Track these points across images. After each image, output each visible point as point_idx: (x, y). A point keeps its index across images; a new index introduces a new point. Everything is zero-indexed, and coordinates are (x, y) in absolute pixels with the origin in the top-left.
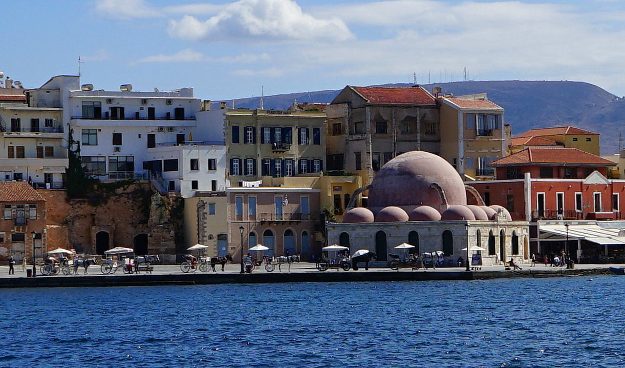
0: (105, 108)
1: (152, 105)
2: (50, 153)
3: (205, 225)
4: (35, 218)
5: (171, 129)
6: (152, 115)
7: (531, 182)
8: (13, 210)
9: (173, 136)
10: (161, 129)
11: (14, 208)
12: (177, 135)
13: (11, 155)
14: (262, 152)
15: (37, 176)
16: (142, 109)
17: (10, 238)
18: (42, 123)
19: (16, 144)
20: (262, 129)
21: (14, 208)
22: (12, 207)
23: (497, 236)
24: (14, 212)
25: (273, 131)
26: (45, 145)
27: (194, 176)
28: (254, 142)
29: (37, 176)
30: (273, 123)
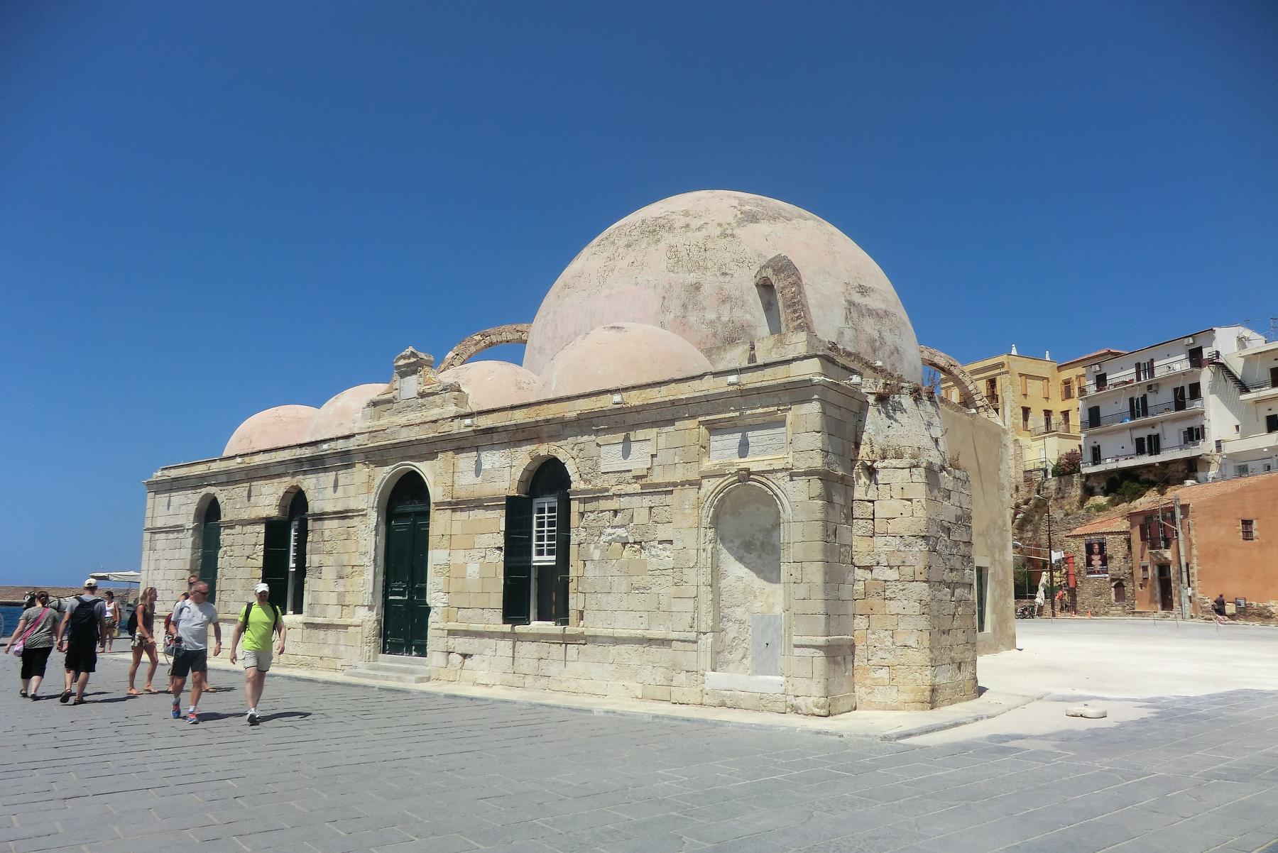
23: (343, 515)
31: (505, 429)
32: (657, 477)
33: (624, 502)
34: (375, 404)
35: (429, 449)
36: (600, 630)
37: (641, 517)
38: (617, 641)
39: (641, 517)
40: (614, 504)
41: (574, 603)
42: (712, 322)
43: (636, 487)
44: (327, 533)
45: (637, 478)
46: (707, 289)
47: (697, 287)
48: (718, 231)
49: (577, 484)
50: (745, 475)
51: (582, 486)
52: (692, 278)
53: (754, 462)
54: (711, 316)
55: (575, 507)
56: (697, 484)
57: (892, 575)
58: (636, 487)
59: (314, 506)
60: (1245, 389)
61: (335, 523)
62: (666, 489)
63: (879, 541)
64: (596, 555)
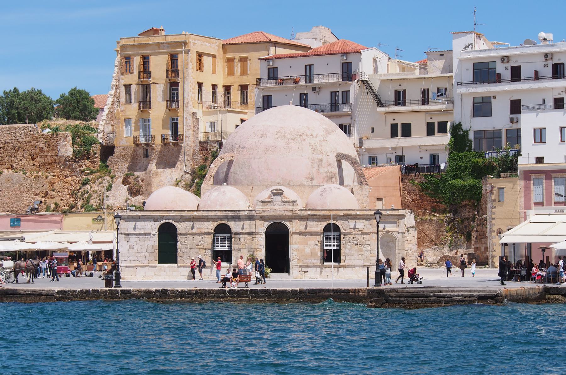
1: (559, 60)
2: (442, 128)
3: (493, 216)
13: (394, 134)
15: (421, 158)
16: (546, 66)
18: (432, 91)
19: (400, 120)
23: (250, 234)
26: (436, 120)
27: (540, 150)
29: (421, 158)
31: (319, 215)
32: (366, 231)
33: (356, 236)
34: (262, 202)
35: (291, 218)
36: (351, 264)
37: (361, 239)
38: (355, 266)
39: (361, 239)
40: (354, 236)
41: (342, 258)
42: (326, 172)
43: (360, 232)
44: (242, 239)
45: (360, 230)
46: (324, 161)
47: (321, 160)
48: (322, 139)
49: (342, 231)
50: (388, 232)
51: (344, 231)
52: (320, 157)
53: (387, 229)
54: (326, 170)
55: (342, 236)
57: (411, 252)
59: (234, 230)
61: (246, 236)
63: (409, 245)
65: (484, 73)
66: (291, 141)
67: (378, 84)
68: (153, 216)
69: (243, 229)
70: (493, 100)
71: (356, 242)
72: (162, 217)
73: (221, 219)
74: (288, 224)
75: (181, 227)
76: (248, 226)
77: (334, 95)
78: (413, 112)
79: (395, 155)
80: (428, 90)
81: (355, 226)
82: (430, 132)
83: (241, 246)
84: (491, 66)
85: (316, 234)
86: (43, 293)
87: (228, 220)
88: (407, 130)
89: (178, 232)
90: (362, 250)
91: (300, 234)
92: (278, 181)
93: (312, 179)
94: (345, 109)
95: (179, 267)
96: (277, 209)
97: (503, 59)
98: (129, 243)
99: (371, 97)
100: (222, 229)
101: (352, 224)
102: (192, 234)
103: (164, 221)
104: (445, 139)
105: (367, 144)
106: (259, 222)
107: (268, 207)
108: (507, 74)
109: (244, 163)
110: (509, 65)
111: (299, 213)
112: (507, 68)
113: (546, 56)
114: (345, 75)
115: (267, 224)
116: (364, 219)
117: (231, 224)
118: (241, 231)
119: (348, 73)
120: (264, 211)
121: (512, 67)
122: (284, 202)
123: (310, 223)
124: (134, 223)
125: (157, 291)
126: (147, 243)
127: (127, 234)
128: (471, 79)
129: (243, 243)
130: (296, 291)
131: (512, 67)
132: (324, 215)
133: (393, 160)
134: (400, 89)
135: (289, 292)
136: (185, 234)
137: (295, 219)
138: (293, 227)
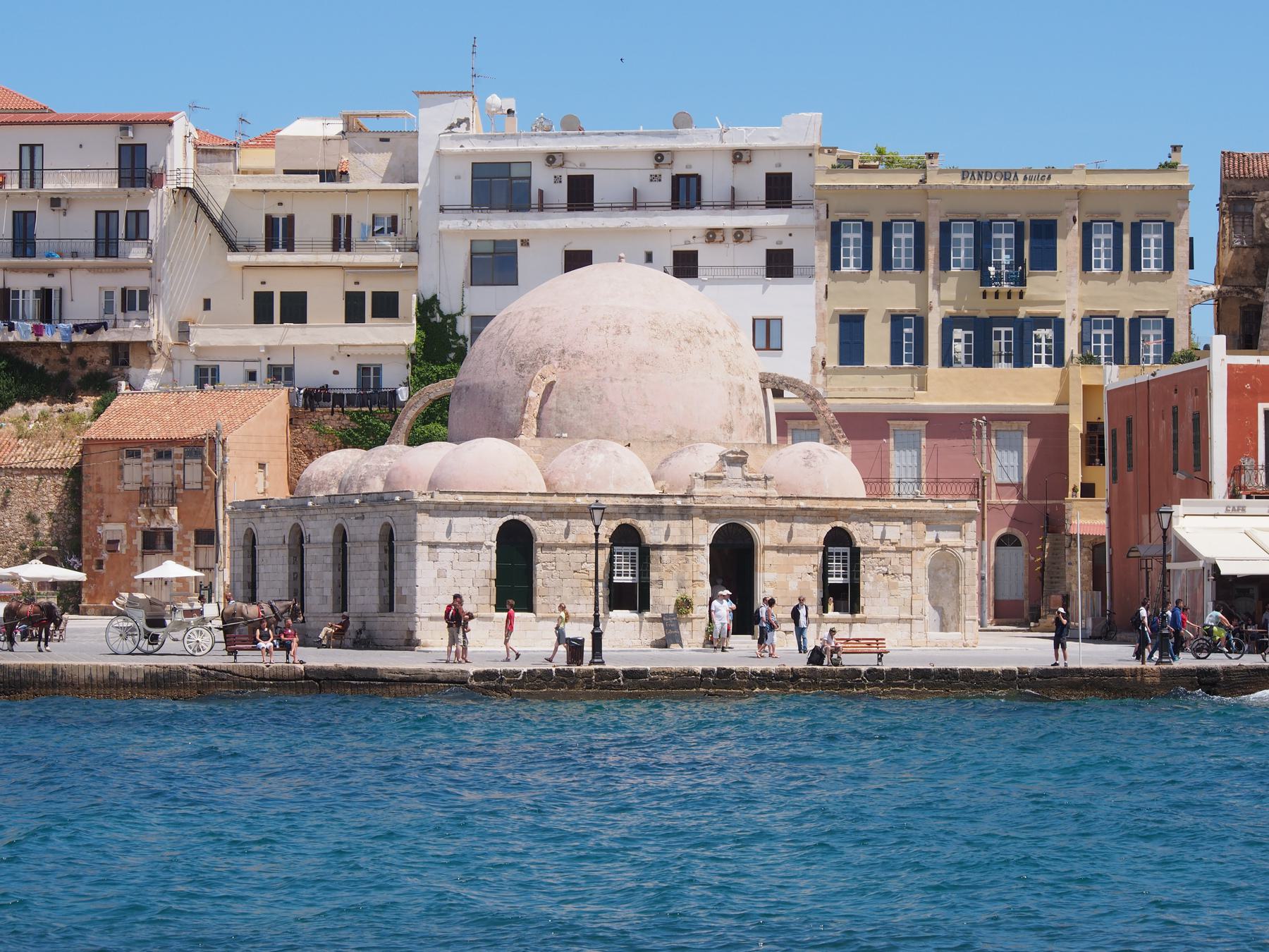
0: (542, 179)
1: (688, 167)
2: (387, 306)
4: (199, 486)
5: (740, 235)
6: (686, 192)
7: (1230, 367)
8: (145, 465)
9: (755, 256)
10: (712, 235)
11: (147, 459)
12: (771, 254)
14: (945, 295)
15: (336, 372)
16: (655, 178)
17: (138, 541)
18: (361, 221)
19: (278, 285)
20: (945, 228)
21: (147, 459)
22: (144, 455)
23: (682, 548)
24: (147, 468)
25: (983, 232)
26: (369, 287)
28: (920, 264)
29: (336, 372)
30: (985, 209)
31: (817, 510)
32: (903, 544)
33: (885, 555)
34: (706, 478)
35: (761, 515)
38: (884, 621)
39: (895, 562)
43: (893, 548)
44: (665, 559)
45: (893, 544)
50: (944, 548)
53: (943, 541)
56: (922, 549)
58: (893, 548)
60: (233, 247)
61: (675, 553)
62: (909, 551)
64: (871, 579)
65: (498, 186)
66: (684, 344)
67: (225, 200)
68: (489, 504)
69: (667, 536)
70: (521, 250)
71: (885, 569)
72: (506, 508)
73: (625, 515)
74: (755, 528)
75: (543, 531)
76: (678, 531)
77: (105, 219)
78: (310, 267)
79: (265, 363)
80: (349, 218)
81: (884, 533)
82: (354, 311)
83: (663, 575)
84: (515, 172)
85: (811, 550)
86: (440, 676)
87: (638, 517)
88: (295, 309)
89: (539, 541)
90: (895, 586)
91: (779, 549)
92: (668, 432)
93: (731, 429)
94: (137, 253)
95: (539, 620)
96: (735, 493)
97: (551, 158)
98: (438, 565)
99: (205, 226)
100: (627, 536)
101: (877, 529)
102: (567, 547)
103: (510, 517)
104: (402, 334)
105: (199, 337)
106: (699, 523)
107: (717, 489)
108: (560, 193)
109: (587, 388)
110: (564, 174)
111: (778, 504)
112: (558, 180)
113: (659, 156)
114: (127, 174)
115: (714, 527)
116: (900, 519)
117: (644, 525)
118: (664, 542)
119: (136, 168)
120: (710, 497)
121: (569, 177)
122: (747, 479)
123: (798, 527)
124: (447, 519)
125: (706, 672)
126: (474, 565)
127: (433, 546)
128: (467, 200)
129: (668, 567)
130: (1011, 672)
131: (569, 177)
132: (827, 510)
133: (262, 374)
134: (280, 213)
135: (998, 675)
136: (551, 547)
137: (770, 517)
138: (765, 534)
